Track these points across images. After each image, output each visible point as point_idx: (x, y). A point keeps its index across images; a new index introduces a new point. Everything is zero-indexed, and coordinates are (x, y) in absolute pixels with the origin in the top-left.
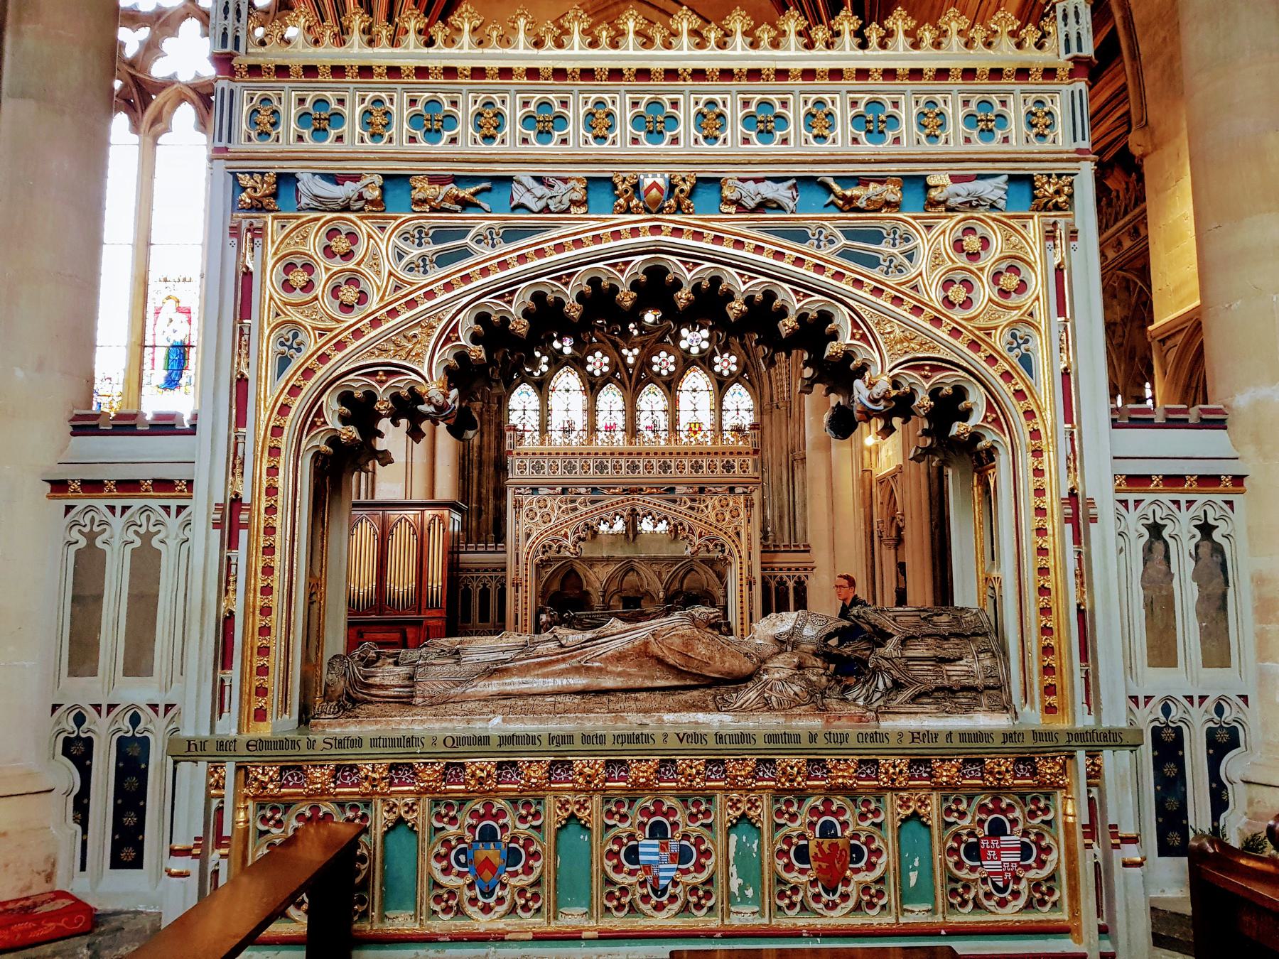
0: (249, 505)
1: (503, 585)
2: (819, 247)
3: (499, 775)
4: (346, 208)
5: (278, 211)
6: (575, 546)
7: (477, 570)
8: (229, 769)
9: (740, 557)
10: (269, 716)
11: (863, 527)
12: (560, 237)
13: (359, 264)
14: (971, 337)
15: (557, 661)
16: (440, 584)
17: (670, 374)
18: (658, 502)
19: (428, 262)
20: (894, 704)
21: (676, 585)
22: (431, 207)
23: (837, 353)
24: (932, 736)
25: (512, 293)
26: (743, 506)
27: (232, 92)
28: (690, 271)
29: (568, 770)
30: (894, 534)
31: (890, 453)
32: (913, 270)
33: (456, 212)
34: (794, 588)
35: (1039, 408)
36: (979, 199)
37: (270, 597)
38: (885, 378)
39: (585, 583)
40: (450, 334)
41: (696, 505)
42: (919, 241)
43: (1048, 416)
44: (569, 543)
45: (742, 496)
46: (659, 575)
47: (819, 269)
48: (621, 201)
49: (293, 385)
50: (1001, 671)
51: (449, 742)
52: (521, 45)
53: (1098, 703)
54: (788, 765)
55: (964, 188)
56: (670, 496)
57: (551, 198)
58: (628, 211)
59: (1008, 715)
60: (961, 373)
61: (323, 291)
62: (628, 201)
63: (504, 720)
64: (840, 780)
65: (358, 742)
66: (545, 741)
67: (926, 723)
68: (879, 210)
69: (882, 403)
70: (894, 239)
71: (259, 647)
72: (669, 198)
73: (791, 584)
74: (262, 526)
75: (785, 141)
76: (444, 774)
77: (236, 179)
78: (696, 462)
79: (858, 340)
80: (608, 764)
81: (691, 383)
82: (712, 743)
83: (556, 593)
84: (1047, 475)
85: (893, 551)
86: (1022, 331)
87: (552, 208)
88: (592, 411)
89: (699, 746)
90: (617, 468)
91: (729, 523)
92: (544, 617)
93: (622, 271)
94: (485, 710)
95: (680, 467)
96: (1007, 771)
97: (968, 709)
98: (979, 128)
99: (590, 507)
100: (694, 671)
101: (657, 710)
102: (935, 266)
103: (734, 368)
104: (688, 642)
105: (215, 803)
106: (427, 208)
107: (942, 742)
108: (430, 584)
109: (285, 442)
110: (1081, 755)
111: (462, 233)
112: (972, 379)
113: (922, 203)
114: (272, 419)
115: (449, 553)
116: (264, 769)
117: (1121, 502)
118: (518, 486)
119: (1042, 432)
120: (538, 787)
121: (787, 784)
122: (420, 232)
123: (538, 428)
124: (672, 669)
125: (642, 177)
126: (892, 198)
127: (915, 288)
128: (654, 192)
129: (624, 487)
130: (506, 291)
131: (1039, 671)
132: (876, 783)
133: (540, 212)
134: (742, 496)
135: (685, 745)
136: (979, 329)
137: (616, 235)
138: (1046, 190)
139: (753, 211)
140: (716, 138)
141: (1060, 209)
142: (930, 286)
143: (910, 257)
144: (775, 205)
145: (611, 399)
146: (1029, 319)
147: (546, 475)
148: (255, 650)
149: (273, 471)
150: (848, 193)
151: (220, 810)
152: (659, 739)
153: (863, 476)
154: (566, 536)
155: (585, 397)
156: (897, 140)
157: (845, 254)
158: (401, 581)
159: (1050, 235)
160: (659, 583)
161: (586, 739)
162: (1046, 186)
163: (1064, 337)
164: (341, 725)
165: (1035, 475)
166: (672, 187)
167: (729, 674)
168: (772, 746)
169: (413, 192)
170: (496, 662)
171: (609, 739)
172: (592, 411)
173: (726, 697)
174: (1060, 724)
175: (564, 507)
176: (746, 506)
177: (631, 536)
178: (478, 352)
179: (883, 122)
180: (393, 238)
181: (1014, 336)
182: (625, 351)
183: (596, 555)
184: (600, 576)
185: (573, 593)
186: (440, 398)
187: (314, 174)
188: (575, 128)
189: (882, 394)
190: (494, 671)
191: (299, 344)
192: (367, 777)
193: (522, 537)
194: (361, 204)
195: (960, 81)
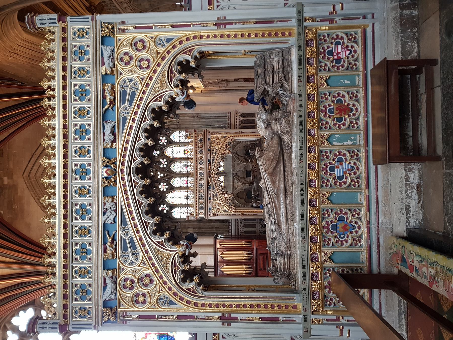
0: (222, 314)
1: (243, 219)
2: (128, 113)
3: (314, 224)
4: (116, 282)
5: (117, 307)
6: (229, 195)
7: (238, 229)
8: (313, 317)
10: (295, 304)
11: (222, 93)
12: (125, 206)
13: (136, 277)
14: (160, 59)
15: (275, 204)
16: (243, 242)
19: (135, 253)
20: (288, 88)
21: (242, 158)
22: (114, 252)
23: (166, 107)
24: (299, 76)
25: (145, 222)
27: (73, 325)
28: (137, 159)
29: (312, 200)
30: (224, 82)
31: (195, 83)
32: (136, 80)
33: (116, 243)
34: (243, 117)
35: (185, 36)
36: (110, 56)
37: (254, 305)
38: (175, 90)
40: (161, 244)
41: (214, 152)
42: (125, 77)
43: (188, 33)
44: (228, 197)
45: (211, 136)
46: (238, 164)
47: (136, 113)
48: (112, 184)
49: (180, 299)
50: (277, 51)
51: (303, 241)
52: (55, 221)
53: (288, 18)
54: (310, 125)
55: (106, 61)
56: (211, 161)
57: (111, 209)
58: (115, 181)
59: (292, 49)
60: (173, 63)
61: (146, 290)
62: (112, 181)
63: (295, 223)
64: (315, 107)
65: (304, 273)
66: (303, 208)
67: (295, 77)
68: (115, 92)
69: (184, 91)
70: (125, 86)
71: (272, 308)
72: (111, 167)
73: (242, 119)
74: (229, 309)
75: (89, 125)
76: (314, 243)
77: (105, 322)
79: (161, 99)
80: (310, 187)
81: (170, 154)
82: (303, 151)
83: (245, 200)
84: (209, 34)
85: (230, 83)
86: (158, 41)
87: (115, 209)
88: (180, 189)
89: (304, 155)
90: (201, 180)
91: (221, 140)
92: (254, 205)
93: (137, 183)
94: (292, 229)
95: (201, 157)
96: (311, 49)
97: (290, 62)
98: (84, 55)
100: (278, 157)
101: (291, 169)
102: (135, 72)
103: (164, 138)
104: (268, 159)
105: (325, 322)
106: (115, 253)
107: (302, 72)
108: (243, 246)
109: (199, 302)
110: (305, 24)
111: (124, 240)
112: (175, 59)
113: (112, 76)
114: (192, 306)
115: (232, 239)
116: (313, 305)
117: (217, 7)
118: (208, 215)
119: (194, 35)
120: (318, 210)
121: (316, 125)
122: (124, 256)
123: (187, 208)
124: (277, 164)
125: (103, 177)
126: (110, 87)
127: (143, 79)
128: (108, 172)
129: (208, 177)
130: (145, 225)
131: (277, 38)
132: (315, 94)
133: (116, 213)
134: (211, 136)
135: (304, 160)
136: (157, 56)
137: (124, 185)
138: (107, 32)
139: (115, 137)
140: (88, 150)
141: (114, 27)
142: (142, 74)
143: (131, 81)
144: (113, 129)
145: (176, 182)
146: (154, 39)
147: (204, 205)
148: (273, 309)
149: (210, 306)
150: (108, 103)
151: (327, 320)
152: (301, 169)
153: (204, 93)
154: (226, 198)
155: (176, 191)
156: (89, 85)
157: (130, 104)
158: (242, 256)
159: (123, 31)
160: (241, 165)
161: (302, 194)
162: (105, 32)
163: (160, 27)
164: (298, 279)
165: (209, 38)
166: (106, 166)
167: (279, 145)
168: (303, 130)
169: (109, 258)
170: (275, 225)
171: (302, 186)
172: (180, 189)
173: (286, 146)
174: (295, 31)
176: (215, 134)
177: (225, 174)
178: (167, 234)
179: (82, 90)
180: (126, 265)
181: (160, 44)
182: (159, 177)
185: (245, 195)
186: (184, 247)
187: (103, 294)
188: (85, 201)
189: (181, 91)
190: (278, 226)
191: (165, 298)
192: (316, 270)
193: (226, 213)
194: (114, 278)
195: (67, 62)
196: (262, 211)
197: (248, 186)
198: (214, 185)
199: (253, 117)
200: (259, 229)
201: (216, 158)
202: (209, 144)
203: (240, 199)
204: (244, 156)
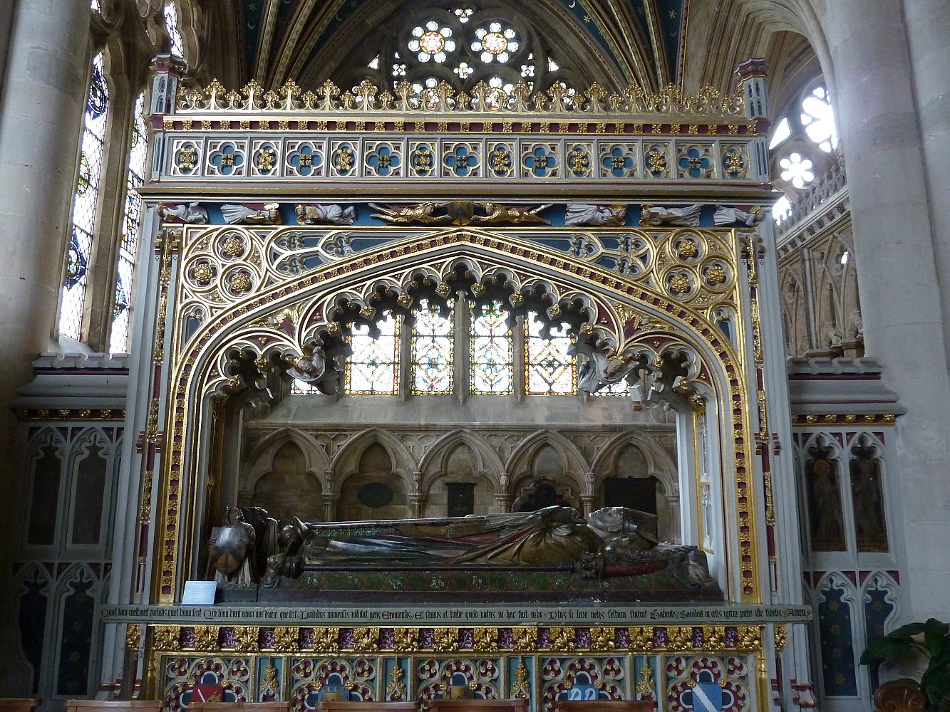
6: (307, 350)
9: (734, 382)
21: (523, 468)
26: (734, 256)
46: (500, 452)
73: (843, 456)
90: (420, 160)
95: (575, 162)
99: (349, 253)
134: (732, 236)
147: (246, 175)
175: (286, 253)
177: (461, 397)
183: (411, 422)
185: (374, 476)
197: (411, 491)
198: (384, 248)
199: (860, 531)
200: (62, 566)
202: (677, 212)
203: (358, 454)
204: (531, 476)
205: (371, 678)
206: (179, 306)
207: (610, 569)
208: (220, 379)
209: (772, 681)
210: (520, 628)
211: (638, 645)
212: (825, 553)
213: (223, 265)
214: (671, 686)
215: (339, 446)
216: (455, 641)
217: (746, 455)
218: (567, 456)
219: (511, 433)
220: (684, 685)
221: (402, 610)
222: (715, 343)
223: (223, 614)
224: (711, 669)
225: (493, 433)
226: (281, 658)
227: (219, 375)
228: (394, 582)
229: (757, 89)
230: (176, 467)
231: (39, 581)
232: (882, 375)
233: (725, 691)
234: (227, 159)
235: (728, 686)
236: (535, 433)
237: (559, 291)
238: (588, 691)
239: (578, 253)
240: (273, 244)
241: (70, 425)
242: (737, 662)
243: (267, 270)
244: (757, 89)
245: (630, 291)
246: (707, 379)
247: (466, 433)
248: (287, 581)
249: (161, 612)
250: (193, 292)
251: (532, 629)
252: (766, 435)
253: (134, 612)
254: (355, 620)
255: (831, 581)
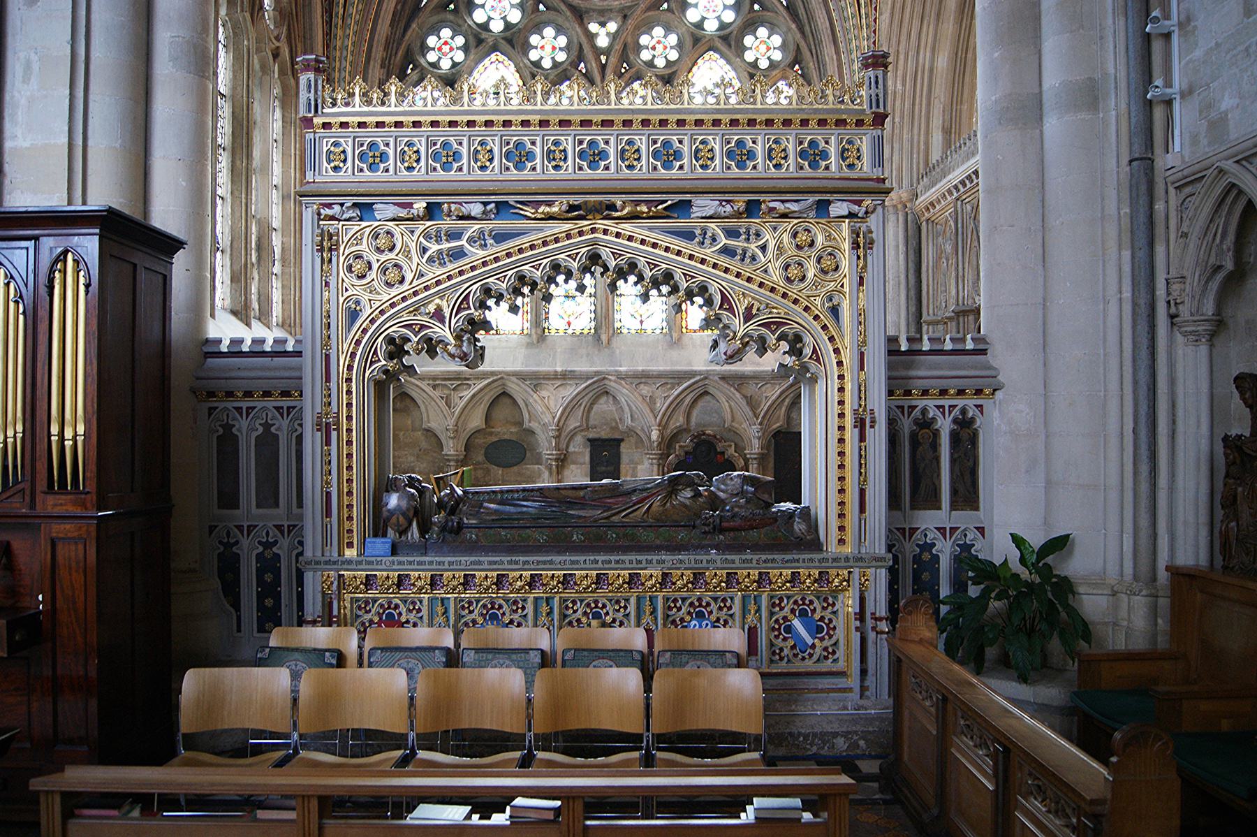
6: (458, 338)
9: (840, 364)
17: (669, 64)
18: (653, 237)
21: (679, 420)
26: (846, 246)
39: (526, 416)
56: (680, 223)
73: (945, 426)
78: (740, 143)
85: (1204, 349)
90: (555, 156)
92: (393, 501)
103: (777, 56)
108: (55, 429)
134: (845, 225)
147: (392, 173)
160: (653, 419)
175: (434, 248)
176: (856, 246)
182: (593, 27)
183: (544, 368)
184: (552, 404)
185: (504, 431)
193: (338, 320)
196: (350, 553)
197: (546, 447)
198: (524, 241)
199: (954, 492)
200: (251, 528)
201: (699, 253)
202: (794, 207)
204: (687, 430)
205: (524, 613)
206: (341, 300)
207: (725, 524)
208: (380, 364)
209: (855, 614)
210: (647, 572)
211: (746, 586)
212: (922, 512)
213: (378, 261)
214: (774, 619)
215: (461, 398)
216: (593, 583)
217: (846, 428)
218: (730, 406)
219: (664, 381)
220: (785, 618)
221: (549, 558)
222: (824, 328)
223: (401, 563)
224: (808, 606)
225: (643, 380)
226: (449, 598)
227: (379, 360)
228: (541, 537)
229: (877, 82)
230: (349, 443)
231: (232, 541)
232: (988, 351)
233: (819, 623)
234: (374, 156)
235: (822, 619)
236: (692, 381)
237: (686, 278)
238: (704, 623)
239: (703, 243)
240: (421, 239)
241: (244, 405)
242: (830, 601)
243: (418, 264)
244: (877, 82)
245: (749, 280)
246: (818, 360)
247: (610, 380)
248: (449, 537)
249: (349, 562)
250: (353, 285)
251: (657, 573)
252: (864, 411)
253: (326, 563)
254: (510, 567)
255: (926, 536)
